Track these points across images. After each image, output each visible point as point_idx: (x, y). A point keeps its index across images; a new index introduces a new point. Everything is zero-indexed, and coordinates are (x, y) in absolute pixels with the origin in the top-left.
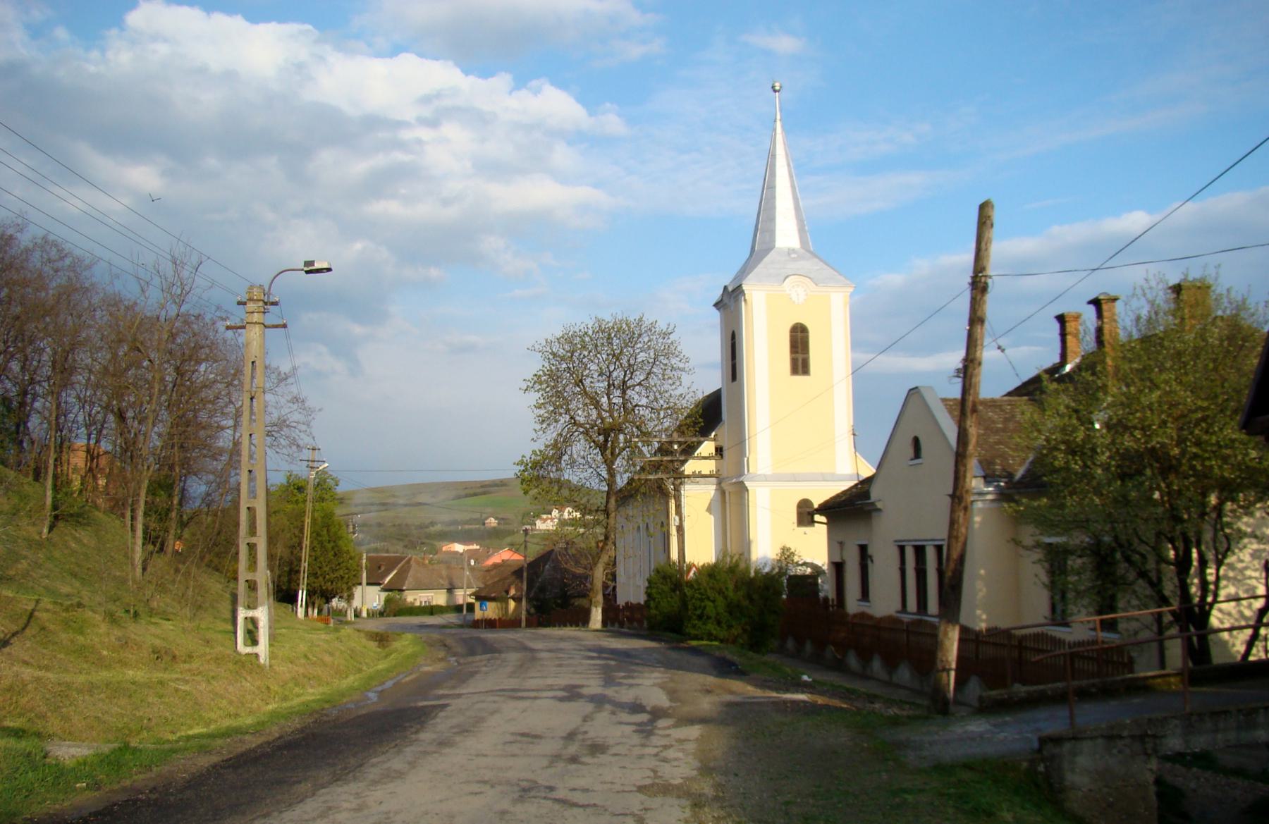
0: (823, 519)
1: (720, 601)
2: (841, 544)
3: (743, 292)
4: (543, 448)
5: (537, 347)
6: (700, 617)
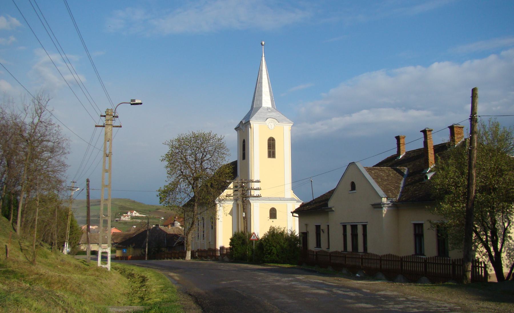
0: (297, 215)
1: (278, 246)
2: (306, 225)
5: (167, 143)
6: (269, 254)
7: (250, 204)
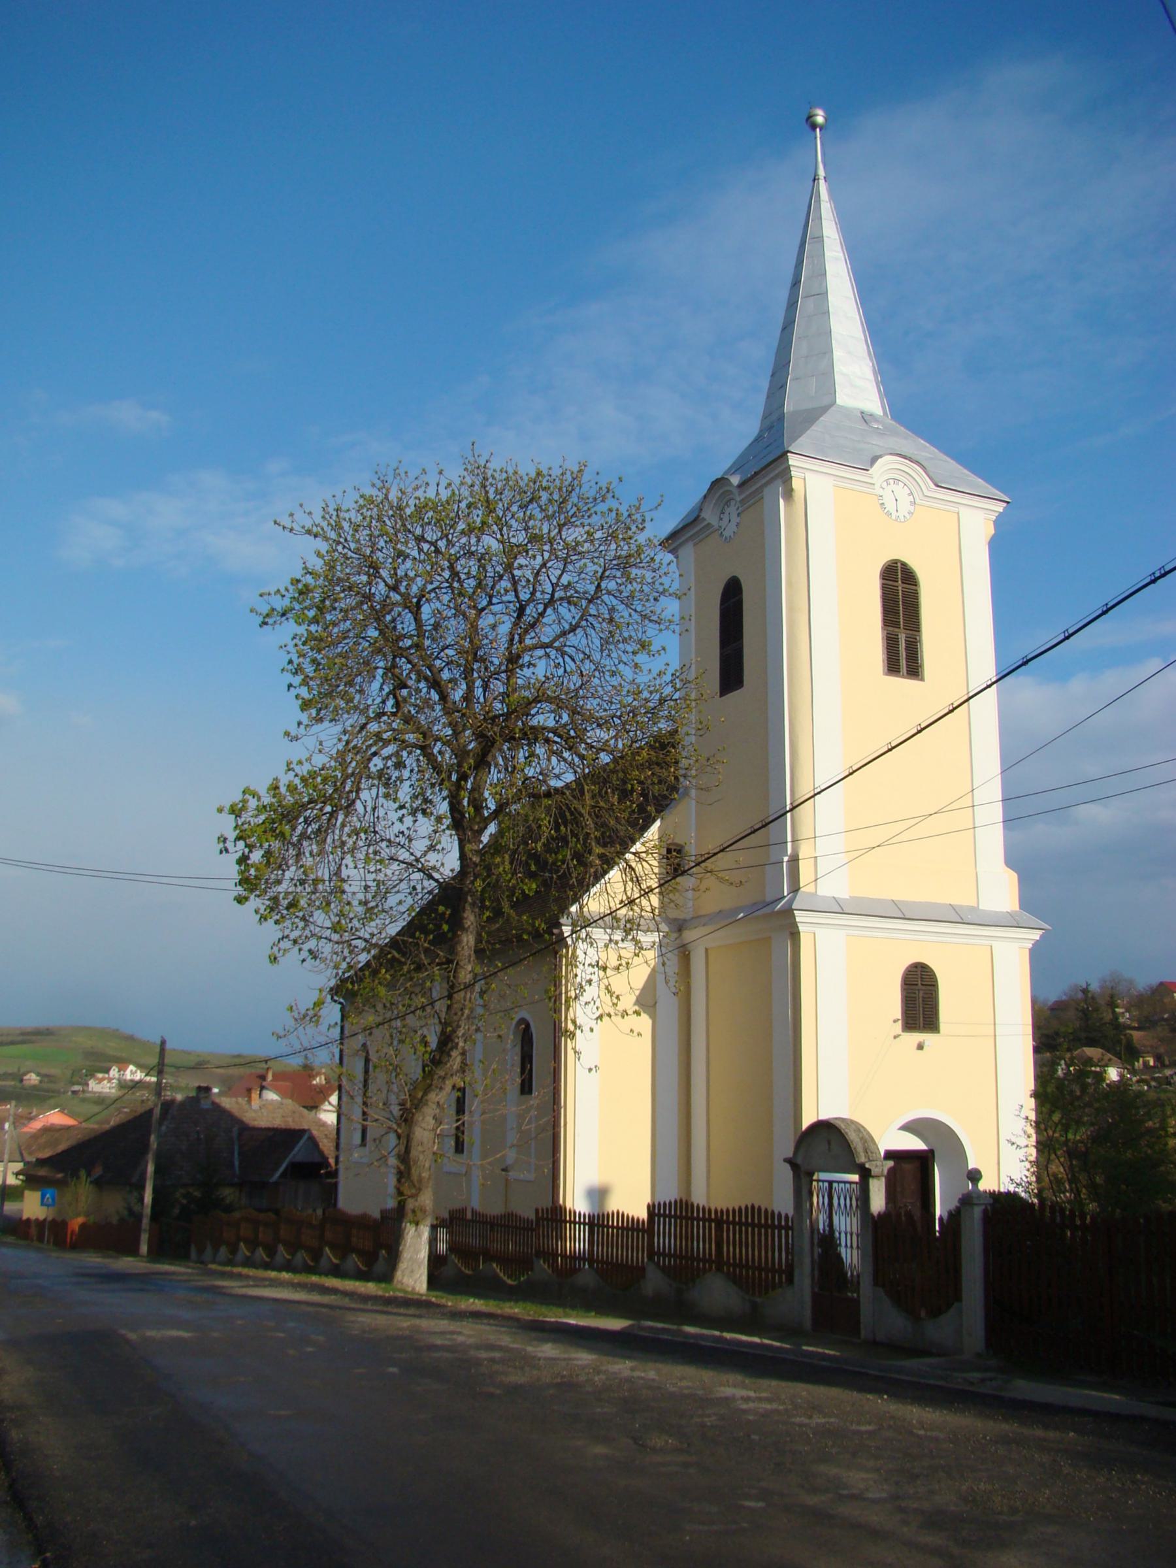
4: (305, 773)
7: (795, 935)
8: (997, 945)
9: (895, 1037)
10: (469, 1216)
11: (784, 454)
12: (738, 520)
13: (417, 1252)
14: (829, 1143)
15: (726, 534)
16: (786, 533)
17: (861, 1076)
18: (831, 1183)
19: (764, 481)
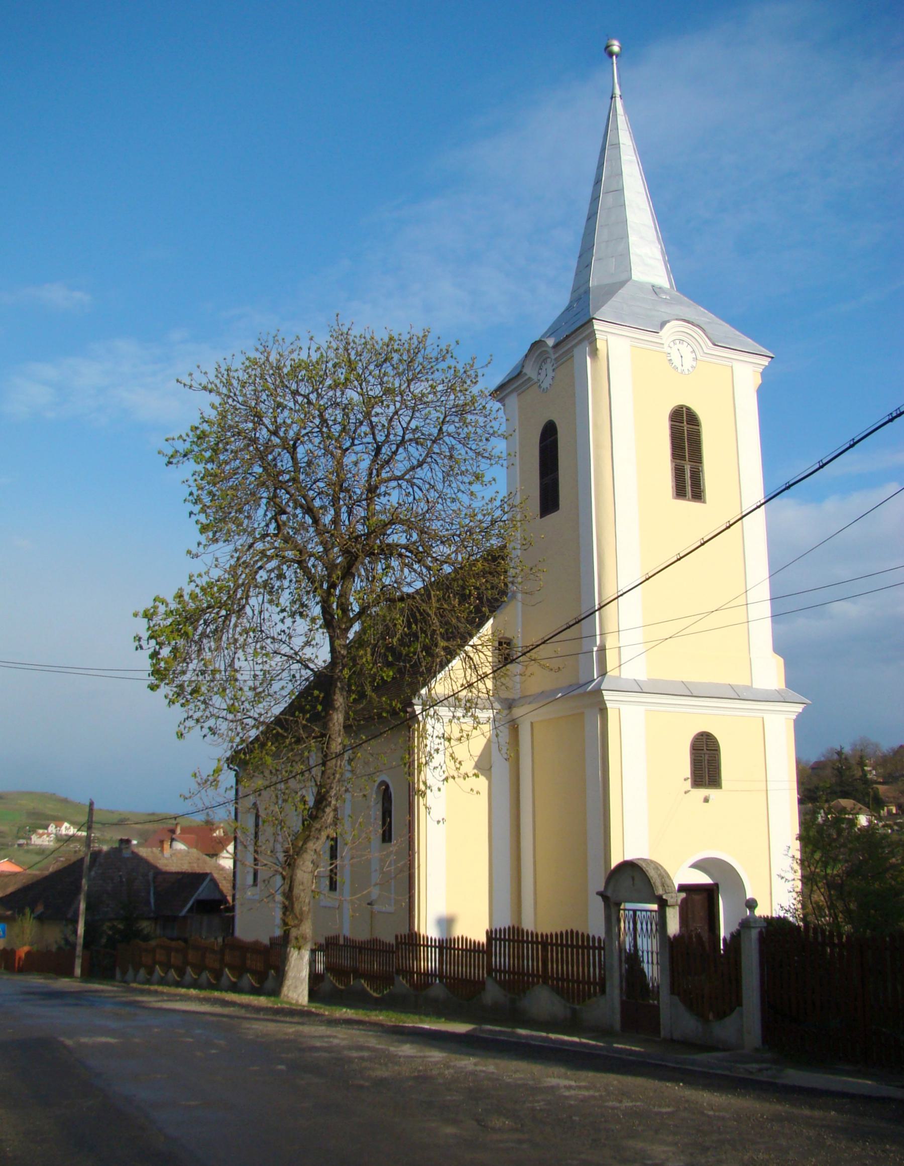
3: (591, 338)
4: (204, 584)
7: (603, 711)
8: (768, 717)
9: (686, 793)
10: (341, 942)
11: (591, 320)
12: (553, 374)
13: (301, 971)
14: (633, 878)
15: (544, 386)
16: (592, 384)
17: (659, 825)
18: (635, 911)
19: (574, 343)
